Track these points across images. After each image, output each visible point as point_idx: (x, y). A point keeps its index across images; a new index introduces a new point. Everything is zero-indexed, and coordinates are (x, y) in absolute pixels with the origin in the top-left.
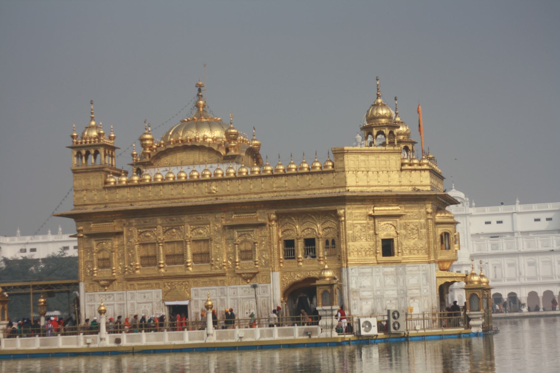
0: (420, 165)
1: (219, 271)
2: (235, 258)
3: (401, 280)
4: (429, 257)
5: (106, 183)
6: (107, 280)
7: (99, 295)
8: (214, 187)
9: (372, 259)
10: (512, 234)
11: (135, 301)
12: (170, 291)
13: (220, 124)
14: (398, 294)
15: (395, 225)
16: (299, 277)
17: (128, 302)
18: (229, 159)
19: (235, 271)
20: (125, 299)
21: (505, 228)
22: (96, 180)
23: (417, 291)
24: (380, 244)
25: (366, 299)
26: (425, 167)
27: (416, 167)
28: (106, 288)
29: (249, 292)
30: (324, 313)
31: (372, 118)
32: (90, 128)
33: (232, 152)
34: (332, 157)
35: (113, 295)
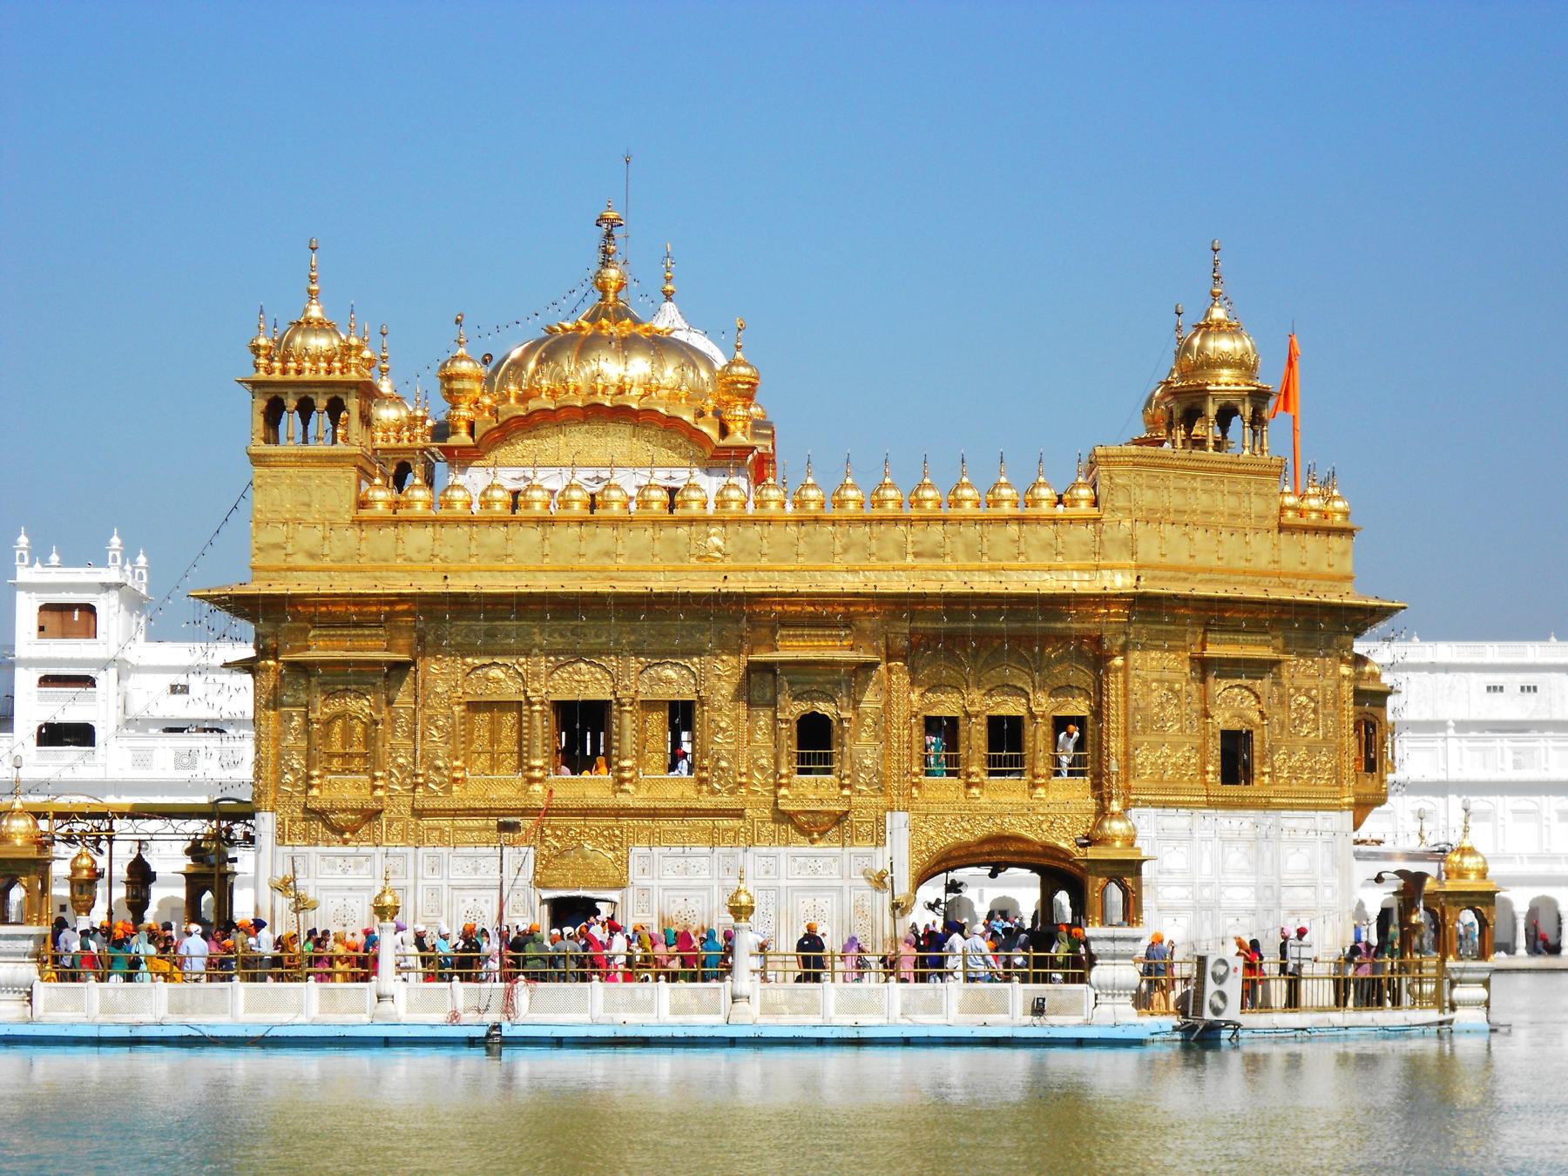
1: (724, 800)
2: (777, 763)
3: (1268, 855)
5: (362, 504)
6: (353, 811)
7: (323, 856)
8: (717, 541)
11: (444, 883)
12: (561, 854)
14: (1258, 899)
15: (1258, 689)
17: (420, 882)
19: (776, 804)
20: (411, 874)
23: (1307, 893)
24: (1215, 748)
28: (347, 836)
29: (815, 871)
33: (738, 437)
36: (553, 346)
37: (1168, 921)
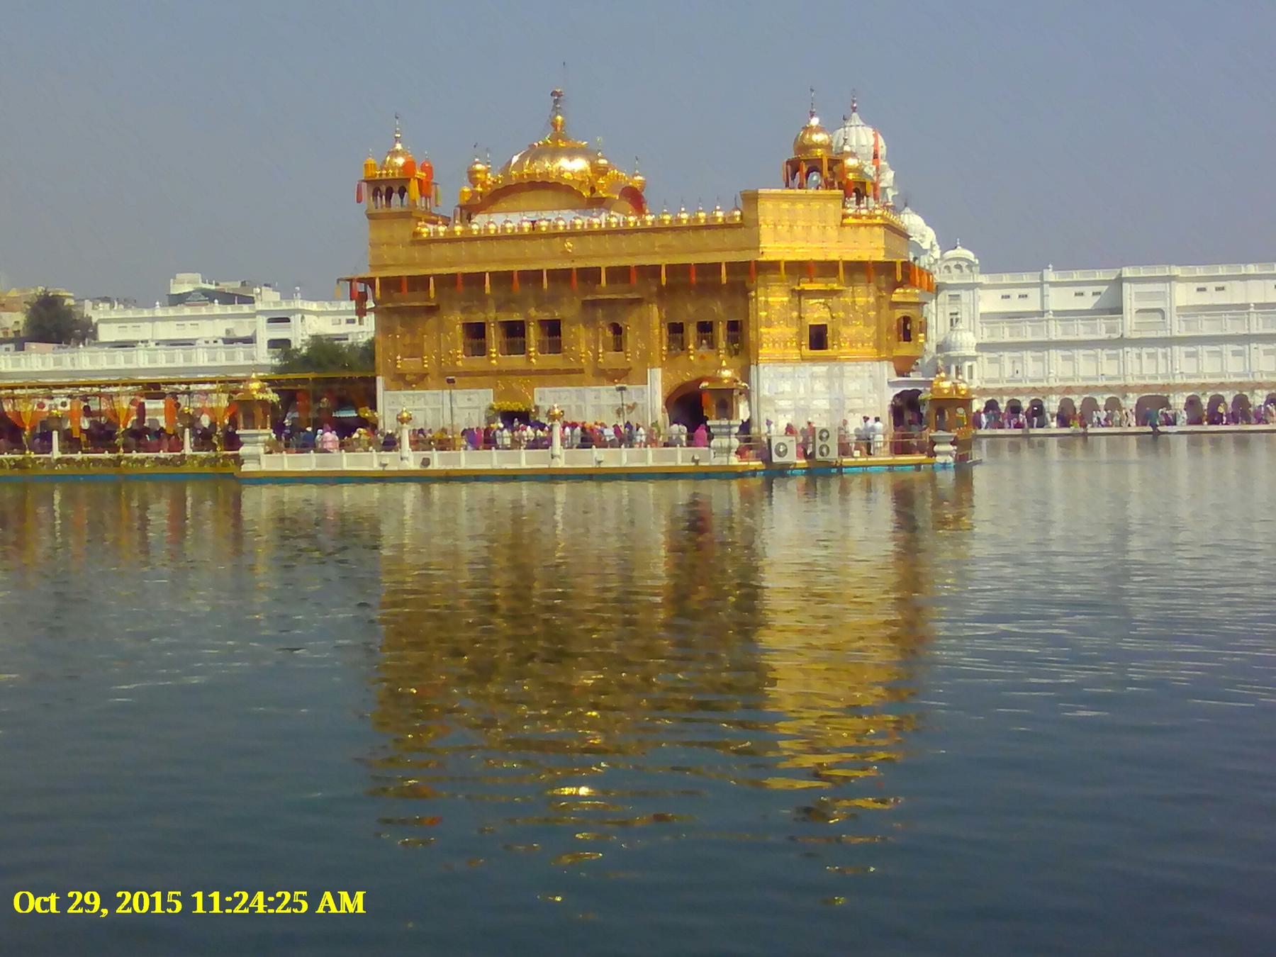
0: (870, 217)
1: (576, 366)
4: (879, 354)
5: (416, 234)
9: (794, 353)
10: (1041, 313)
13: (583, 152)
16: (688, 376)
18: (598, 203)
21: (1032, 305)
22: (401, 231)
23: (859, 401)
25: (785, 412)
26: (879, 220)
27: (864, 220)
30: (718, 430)
31: (803, 148)
32: (395, 154)
34: (740, 204)
35: (424, 395)
36: (535, 154)
37: (781, 416)
